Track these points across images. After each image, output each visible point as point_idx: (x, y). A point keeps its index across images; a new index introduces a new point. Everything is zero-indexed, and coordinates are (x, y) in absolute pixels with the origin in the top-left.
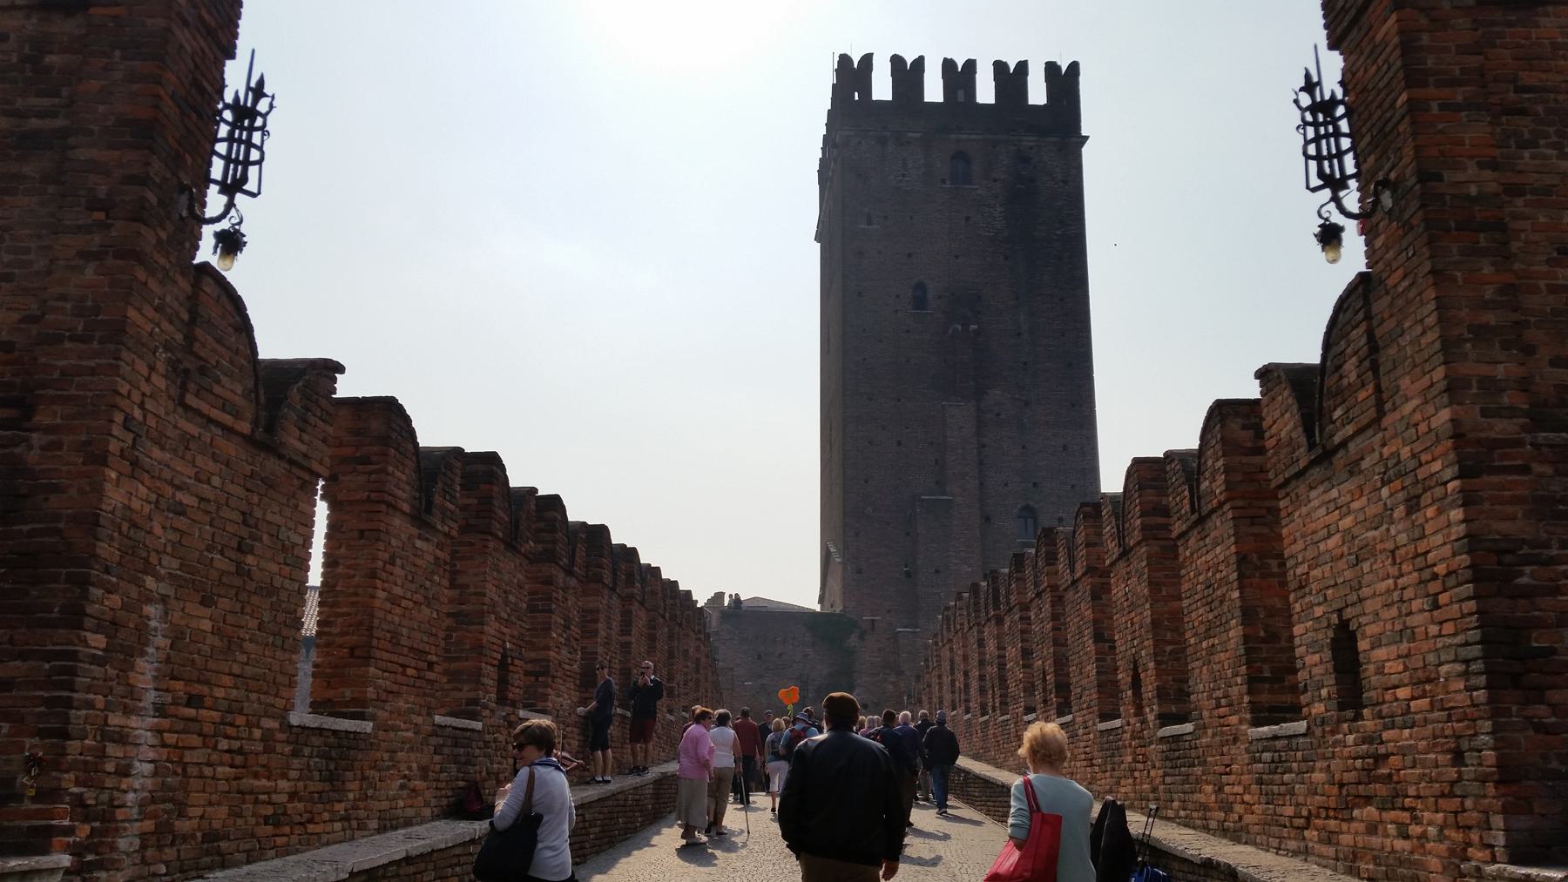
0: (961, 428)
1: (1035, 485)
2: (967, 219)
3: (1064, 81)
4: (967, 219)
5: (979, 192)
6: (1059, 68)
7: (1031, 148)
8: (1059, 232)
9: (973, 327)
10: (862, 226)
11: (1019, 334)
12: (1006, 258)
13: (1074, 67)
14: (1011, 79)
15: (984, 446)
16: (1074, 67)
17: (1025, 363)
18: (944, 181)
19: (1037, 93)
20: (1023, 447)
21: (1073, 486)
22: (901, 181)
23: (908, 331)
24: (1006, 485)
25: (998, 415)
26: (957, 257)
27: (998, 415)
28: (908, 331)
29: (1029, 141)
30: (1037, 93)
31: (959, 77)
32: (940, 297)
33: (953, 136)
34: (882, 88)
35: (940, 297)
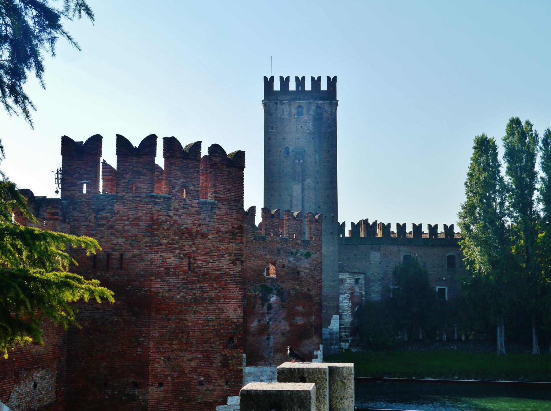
0: (297, 191)
1: (319, 207)
2: (302, 127)
3: (332, 82)
4: (302, 127)
5: (305, 118)
6: (330, 78)
7: (321, 104)
8: (329, 130)
9: (301, 161)
10: (270, 130)
11: (316, 162)
12: (313, 139)
13: (335, 78)
14: (316, 82)
15: (304, 196)
16: (335, 78)
17: (317, 171)
18: (295, 115)
19: (324, 87)
20: (316, 196)
21: (330, 207)
22: (282, 116)
23: (283, 162)
24: (311, 207)
25: (309, 186)
26: (298, 139)
27: (309, 186)
28: (283, 162)
29: (320, 102)
30: (324, 87)
31: (300, 82)
32: (293, 151)
33: (297, 101)
34: (277, 87)
35: (293, 151)
